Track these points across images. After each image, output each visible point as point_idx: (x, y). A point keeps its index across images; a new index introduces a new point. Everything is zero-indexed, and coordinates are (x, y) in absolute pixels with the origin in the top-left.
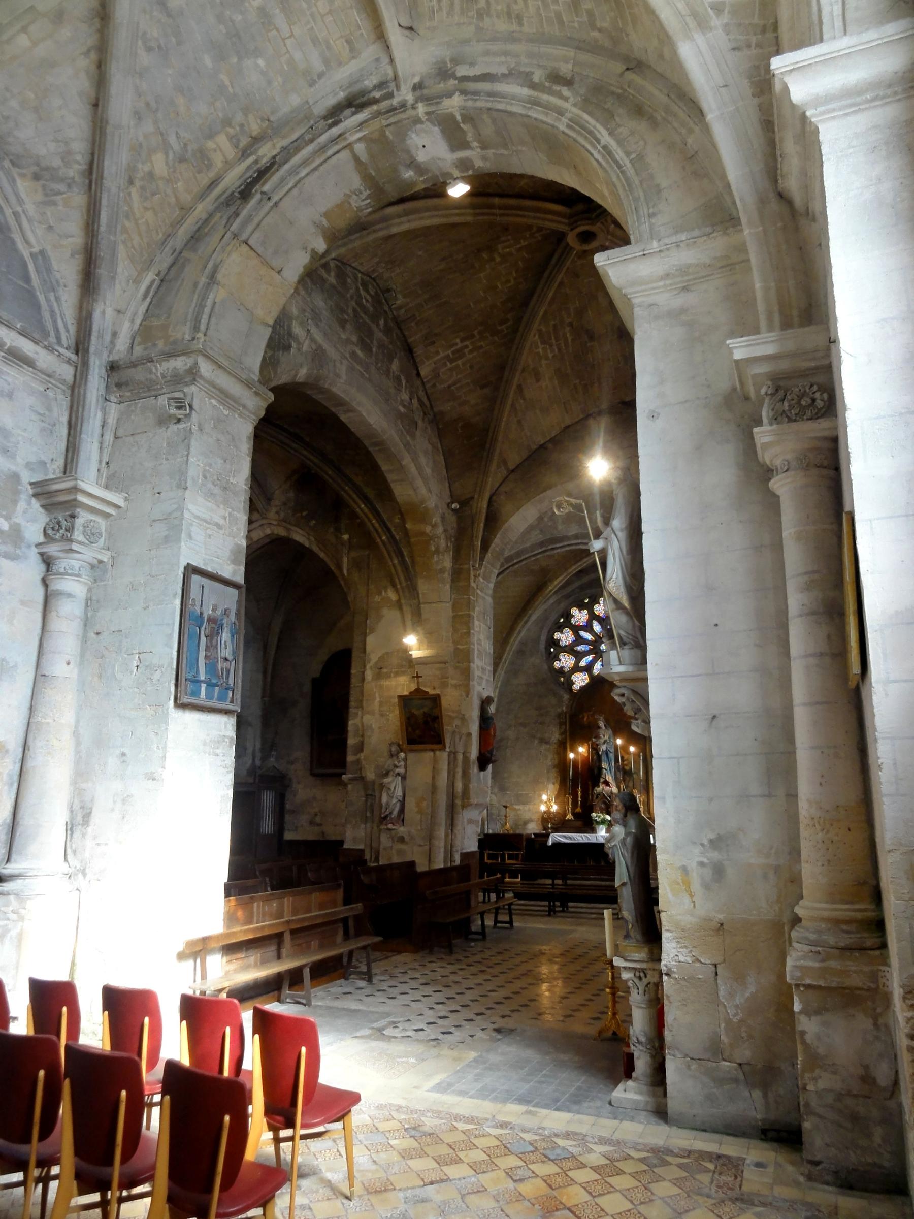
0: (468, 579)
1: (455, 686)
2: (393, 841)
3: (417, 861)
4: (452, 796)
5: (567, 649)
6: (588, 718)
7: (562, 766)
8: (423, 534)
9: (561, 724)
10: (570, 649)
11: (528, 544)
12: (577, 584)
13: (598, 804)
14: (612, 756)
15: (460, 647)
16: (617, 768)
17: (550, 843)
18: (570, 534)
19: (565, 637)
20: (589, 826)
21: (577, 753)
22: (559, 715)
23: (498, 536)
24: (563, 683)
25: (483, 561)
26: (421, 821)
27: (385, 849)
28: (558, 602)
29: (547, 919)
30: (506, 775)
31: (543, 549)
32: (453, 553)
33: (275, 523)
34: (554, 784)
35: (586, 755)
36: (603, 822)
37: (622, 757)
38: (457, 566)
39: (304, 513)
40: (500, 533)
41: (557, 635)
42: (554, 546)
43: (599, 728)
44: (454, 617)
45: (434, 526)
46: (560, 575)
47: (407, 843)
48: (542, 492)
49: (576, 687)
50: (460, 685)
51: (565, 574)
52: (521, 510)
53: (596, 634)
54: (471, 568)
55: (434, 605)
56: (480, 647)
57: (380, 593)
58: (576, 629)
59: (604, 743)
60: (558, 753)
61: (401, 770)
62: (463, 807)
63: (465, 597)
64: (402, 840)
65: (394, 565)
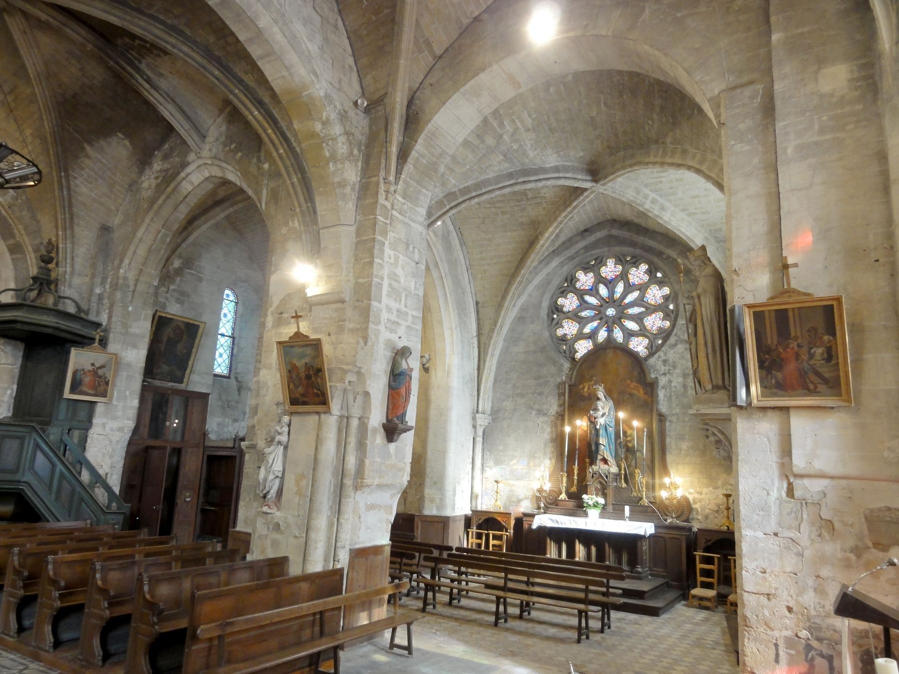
0: (377, 193)
1: (352, 331)
2: (268, 529)
3: (291, 558)
4: (341, 473)
5: (569, 315)
6: (589, 388)
7: (559, 439)
8: (313, 135)
10: (575, 316)
11: (491, 175)
12: (582, 244)
13: (593, 485)
14: (611, 430)
15: (361, 281)
17: (534, 526)
18: (548, 166)
19: (569, 303)
20: (579, 508)
22: (561, 385)
23: (420, 141)
26: (299, 504)
27: (260, 537)
28: (562, 265)
29: (489, 634)
30: (501, 448)
31: (512, 182)
32: (362, 163)
33: (209, 162)
34: (550, 459)
36: (596, 505)
37: (625, 433)
38: (364, 180)
39: (233, 146)
40: (423, 136)
41: (561, 301)
42: (526, 179)
43: (598, 399)
44: (357, 244)
45: (326, 123)
47: (282, 533)
48: (474, 77)
49: (578, 356)
50: (357, 329)
51: (555, 224)
52: (447, 104)
53: (603, 299)
54: (382, 181)
55: (332, 230)
56: (393, 283)
57: (287, 224)
58: (580, 294)
59: (603, 416)
60: (556, 425)
61: (284, 438)
62: (357, 488)
63: (372, 217)
64: (277, 527)
65: (293, 184)
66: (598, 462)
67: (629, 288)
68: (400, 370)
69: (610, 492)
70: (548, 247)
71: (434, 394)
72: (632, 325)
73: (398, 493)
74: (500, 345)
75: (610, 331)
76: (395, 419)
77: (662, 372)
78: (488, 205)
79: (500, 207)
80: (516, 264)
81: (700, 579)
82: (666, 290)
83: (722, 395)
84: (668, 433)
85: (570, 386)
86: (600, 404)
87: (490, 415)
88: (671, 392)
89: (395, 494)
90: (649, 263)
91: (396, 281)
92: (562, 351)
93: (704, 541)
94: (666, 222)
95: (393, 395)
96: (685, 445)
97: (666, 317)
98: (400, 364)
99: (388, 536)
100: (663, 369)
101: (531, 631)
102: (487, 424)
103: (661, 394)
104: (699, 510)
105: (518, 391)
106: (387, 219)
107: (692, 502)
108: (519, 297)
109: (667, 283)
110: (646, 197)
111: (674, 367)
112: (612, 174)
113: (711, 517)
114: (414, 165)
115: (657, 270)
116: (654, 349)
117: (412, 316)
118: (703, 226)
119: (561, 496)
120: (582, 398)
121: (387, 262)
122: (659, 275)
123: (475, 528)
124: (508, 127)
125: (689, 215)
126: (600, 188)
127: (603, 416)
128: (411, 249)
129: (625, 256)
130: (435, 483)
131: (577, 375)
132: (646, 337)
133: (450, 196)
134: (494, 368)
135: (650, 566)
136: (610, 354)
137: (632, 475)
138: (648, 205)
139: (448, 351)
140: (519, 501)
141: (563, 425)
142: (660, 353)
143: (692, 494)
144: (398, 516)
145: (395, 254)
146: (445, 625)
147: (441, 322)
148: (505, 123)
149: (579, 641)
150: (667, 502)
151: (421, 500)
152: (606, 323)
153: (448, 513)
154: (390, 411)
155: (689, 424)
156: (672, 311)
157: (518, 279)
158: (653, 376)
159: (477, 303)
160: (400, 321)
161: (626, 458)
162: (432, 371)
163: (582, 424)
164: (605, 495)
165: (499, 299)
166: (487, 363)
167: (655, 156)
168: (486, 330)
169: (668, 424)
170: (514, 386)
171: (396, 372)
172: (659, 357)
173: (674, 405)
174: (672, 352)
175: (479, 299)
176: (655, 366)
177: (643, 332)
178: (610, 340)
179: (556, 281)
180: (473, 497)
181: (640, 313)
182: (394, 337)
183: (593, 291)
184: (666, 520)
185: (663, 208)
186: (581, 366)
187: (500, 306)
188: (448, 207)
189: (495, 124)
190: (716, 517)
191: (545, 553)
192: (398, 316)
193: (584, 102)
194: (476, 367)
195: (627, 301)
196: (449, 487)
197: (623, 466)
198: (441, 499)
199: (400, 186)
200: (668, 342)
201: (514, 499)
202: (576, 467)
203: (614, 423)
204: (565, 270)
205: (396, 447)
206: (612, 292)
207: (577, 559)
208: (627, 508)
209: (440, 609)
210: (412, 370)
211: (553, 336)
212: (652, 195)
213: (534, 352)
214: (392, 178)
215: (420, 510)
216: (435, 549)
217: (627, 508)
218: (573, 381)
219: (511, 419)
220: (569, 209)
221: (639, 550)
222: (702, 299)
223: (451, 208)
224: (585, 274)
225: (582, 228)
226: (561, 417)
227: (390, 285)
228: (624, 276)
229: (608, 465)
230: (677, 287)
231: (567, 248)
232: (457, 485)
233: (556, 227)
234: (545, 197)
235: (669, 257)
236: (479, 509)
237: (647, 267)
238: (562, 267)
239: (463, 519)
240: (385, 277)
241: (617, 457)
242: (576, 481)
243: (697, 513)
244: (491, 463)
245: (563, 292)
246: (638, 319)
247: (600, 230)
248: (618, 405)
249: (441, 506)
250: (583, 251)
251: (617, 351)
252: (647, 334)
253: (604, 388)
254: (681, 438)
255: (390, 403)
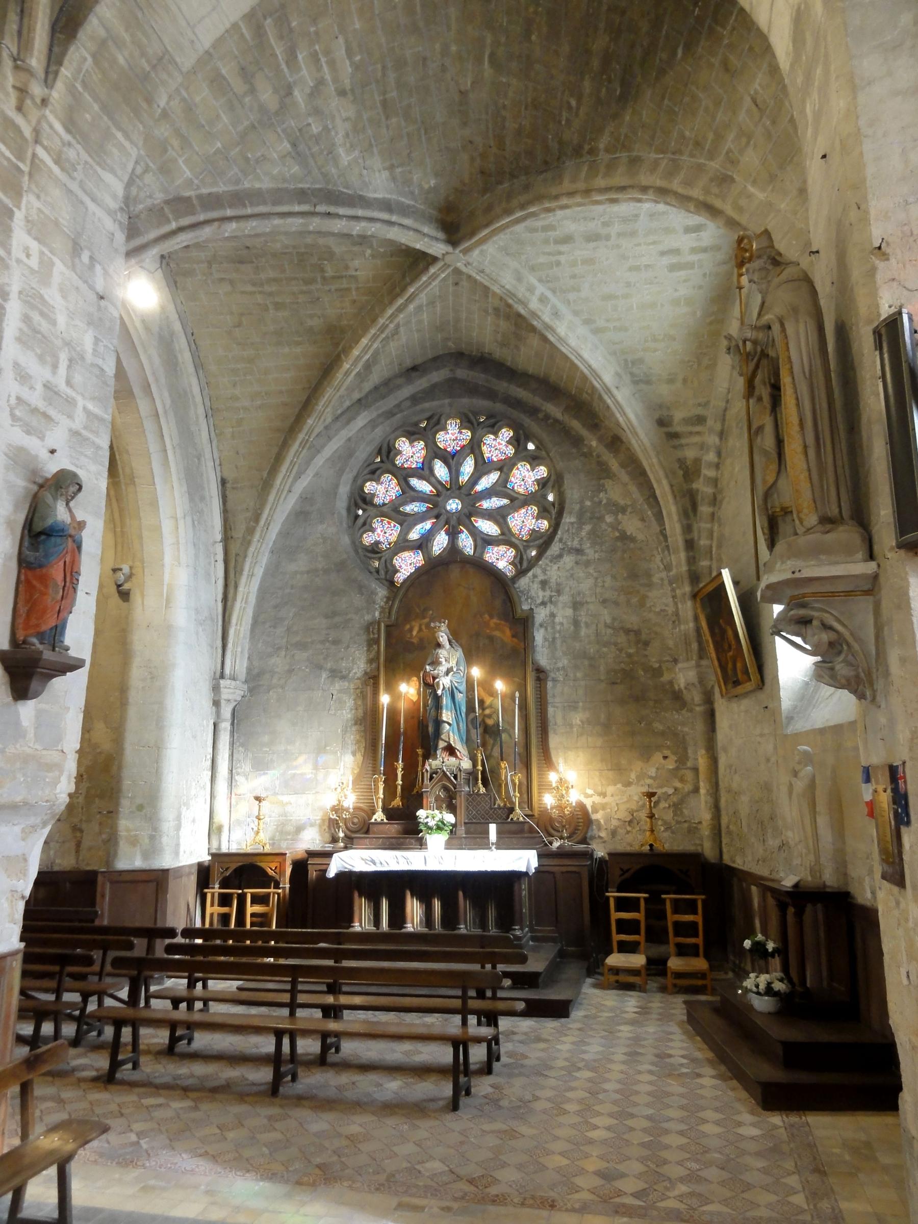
5: (385, 509)
6: (420, 630)
9: (372, 642)
10: (393, 512)
11: (265, 184)
12: (407, 391)
13: (432, 791)
14: (460, 697)
16: (472, 722)
17: (331, 873)
18: (372, 195)
21: (396, 697)
22: (369, 627)
24: (378, 571)
25: (60, 63)
28: (373, 424)
30: (266, 738)
31: (305, 208)
34: (354, 754)
35: (415, 698)
36: (440, 828)
37: (481, 702)
41: (369, 487)
42: (332, 209)
43: (439, 645)
46: (365, 330)
49: (400, 577)
53: (440, 482)
56: (36, 317)
58: (403, 476)
59: (447, 673)
60: (363, 696)
66: (439, 752)
67: (483, 467)
68: (50, 522)
69: (461, 802)
70: (350, 390)
71: (140, 641)
72: (488, 527)
73: (44, 824)
74: (264, 559)
75: (453, 535)
76: (35, 640)
77: (539, 601)
78: (250, 288)
79: (271, 294)
80: (297, 410)
81: (616, 937)
82: (542, 471)
83: (847, 534)
84: (550, 700)
85: (387, 626)
86: (442, 653)
87: (246, 681)
88: (554, 633)
89: (34, 828)
90: (516, 426)
91: (42, 314)
92: (373, 570)
93: (618, 872)
94: (560, 339)
95: (28, 582)
96: (577, 718)
97: (544, 512)
98: (52, 509)
99: (16, 930)
100: (541, 595)
101: (350, 1095)
102: (239, 698)
103: (539, 636)
104: (602, 822)
105: (298, 638)
106: (21, 158)
107: (590, 809)
108: (298, 476)
109: (543, 459)
110: (531, 289)
111: (559, 592)
112: (487, 225)
113: (621, 831)
114: (94, 56)
115: (528, 439)
116: (525, 565)
117: (85, 408)
118: (615, 353)
119: (375, 817)
120: (409, 647)
121: (18, 261)
122: (531, 446)
123: (217, 886)
124: (304, 72)
125: (596, 331)
126: (458, 259)
127: (447, 673)
128: (85, 257)
129: (476, 414)
130: (140, 808)
131: (399, 608)
132: (511, 545)
133: (180, 204)
134: (253, 599)
135: (531, 922)
136: (455, 572)
137: (495, 772)
138: (534, 305)
139: (168, 559)
140: (299, 829)
141: (376, 694)
142: (537, 570)
143: (591, 796)
144: (44, 880)
145: (42, 253)
146: (158, 1114)
147: (154, 504)
148: (300, 57)
149: (454, 1105)
150: (555, 813)
151: (111, 842)
152: (447, 523)
153: (166, 861)
154: (20, 621)
155: (583, 683)
156: (553, 504)
157: (301, 436)
158: (525, 607)
159: (223, 482)
160: (52, 412)
161: (484, 745)
162: (136, 597)
163: (409, 690)
164: (452, 809)
165: (265, 474)
166: (241, 589)
167: (574, 180)
168: (239, 532)
169: (550, 684)
170: (288, 629)
171: (39, 526)
172: (535, 576)
173: (559, 653)
174: (555, 567)
175: (226, 475)
176: (529, 590)
177: (506, 538)
178: (453, 549)
179: (363, 453)
180: (214, 830)
181: (501, 507)
182: (37, 447)
183: (425, 472)
184: (551, 843)
185: (556, 314)
186: (405, 594)
187: (266, 485)
188: (174, 225)
189: (279, 50)
190: (628, 832)
191: (350, 920)
192: (49, 401)
193: (454, 48)
194: (220, 597)
195: (479, 488)
196: (167, 813)
197: (480, 758)
198: (152, 838)
199: (58, 93)
200: (549, 553)
201: (289, 828)
202: (400, 765)
203: (464, 684)
204: (379, 433)
205: (39, 714)
206: (454, 472)
207: (409, 928)
208: (493, 828)
209: (150, 1068)
210: (81, 525)
211: (357, 544)
212: (540, 289)
213: (326, 571)
214: (36, 61)
215: (109, 861)
216: (135, 936)
217: (493, 828)
218: (393, 617)
219: (282, 688)
220: (400, 301)
221: (517, 898)
222: (787, 325)
223: (181, 229)
224: (411, 442)
225: (408, 363)
226: (372, 681)
227: (26, 319)
228: (475, 446)
229: (456, 757)
230: (560, 465)
231: (383, 397)
232: (184, 809)
233: (374, 338)
234: (355, 278)
235: (547, 417)
236: (224, 850)
237: (512, 434)
238: (374, 427)
239: (195, 871)
240: (14, 295)
241: (468, 742)
242: (399, 788)
243: (599, 829)
244: (247, 767)
245: (373, 472)
246: (499, 516)
247: (437, 369)
248: (470, 657)
249: (153, 848)
250: (408, 403)
251: (468, 566)
252: (514, 540)
253: (449, 626)
254: (572, 706)
255: (22, 597)
